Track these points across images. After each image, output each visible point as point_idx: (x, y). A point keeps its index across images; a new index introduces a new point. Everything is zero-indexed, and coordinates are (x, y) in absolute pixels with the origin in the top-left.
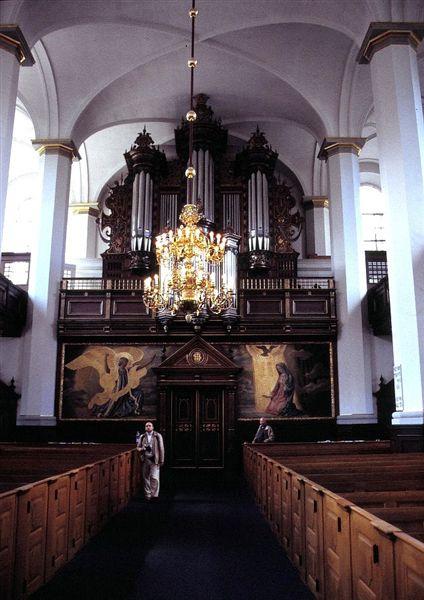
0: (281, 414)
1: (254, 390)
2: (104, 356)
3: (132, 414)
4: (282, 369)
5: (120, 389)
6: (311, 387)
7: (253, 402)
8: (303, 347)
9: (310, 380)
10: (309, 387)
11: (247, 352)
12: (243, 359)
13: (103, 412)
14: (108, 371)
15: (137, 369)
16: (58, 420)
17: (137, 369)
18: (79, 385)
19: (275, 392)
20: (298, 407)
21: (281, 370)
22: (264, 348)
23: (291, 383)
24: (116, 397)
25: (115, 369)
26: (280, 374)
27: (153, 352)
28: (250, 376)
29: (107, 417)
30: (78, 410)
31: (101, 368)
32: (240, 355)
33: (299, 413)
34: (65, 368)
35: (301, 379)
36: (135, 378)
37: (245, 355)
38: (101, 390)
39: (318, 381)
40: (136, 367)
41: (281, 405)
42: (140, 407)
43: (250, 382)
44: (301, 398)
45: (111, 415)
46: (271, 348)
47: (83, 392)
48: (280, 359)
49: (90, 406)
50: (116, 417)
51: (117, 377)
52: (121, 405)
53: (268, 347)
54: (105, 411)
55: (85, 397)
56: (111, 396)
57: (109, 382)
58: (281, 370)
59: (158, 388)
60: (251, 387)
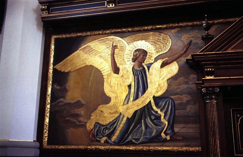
2: (109, 51)
3: (157, 139)
5: (136, 97)
13: (110, 136)
14: (116, 70)
15: (163, 65)
16: (41, 147)
17: (163, 65)
18: (74, 94)
24: (130, 110)
25: (127, 65)
27: (185, 38)
29: (115, 144)
30: (71, 132)
31: (105, 67)
34: (54, 70)
36: (159, 78)
38: (107, 100)
40: (160, 62)
42: (171, 126)
45: (121, 140)
47: (78, 104)
49: (90, 126)
50: (130, 143)
51: (131, 79)
52: (139, 122)
54: (113, 133)
55: (82, 111)
56: (121, 109)
57: (117, 87)
59: (200, 96)
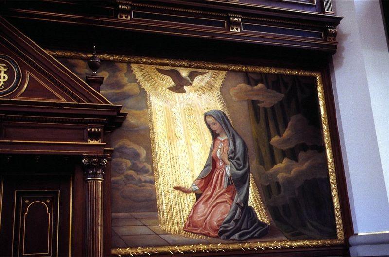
0: (223, 233)
1: (153, 172)
4: (218, 124)
6: (288, 169)
7: (150, 204)
8: (263, 78)
9: (284, 154)
10: (283, 170)
11: (135, 81)
12: (126, 96)
19: (207, 179)
20: (262, 216)
21: (217, 127)
22: (176, 75)
23: (241, 159)
26: (215, 135)
28: (145, 136)
32: (118, 85)
33: (265, 232)
35: (265, 152)
37: (130, 87)
39: (302, 155)
41: (221, 212)
43: (143, 153)
44: (267, 192)
46: (192, 76)
48: (213, 102)
53: (184, 73)
58: (217, 127)
60: (147, 166)
